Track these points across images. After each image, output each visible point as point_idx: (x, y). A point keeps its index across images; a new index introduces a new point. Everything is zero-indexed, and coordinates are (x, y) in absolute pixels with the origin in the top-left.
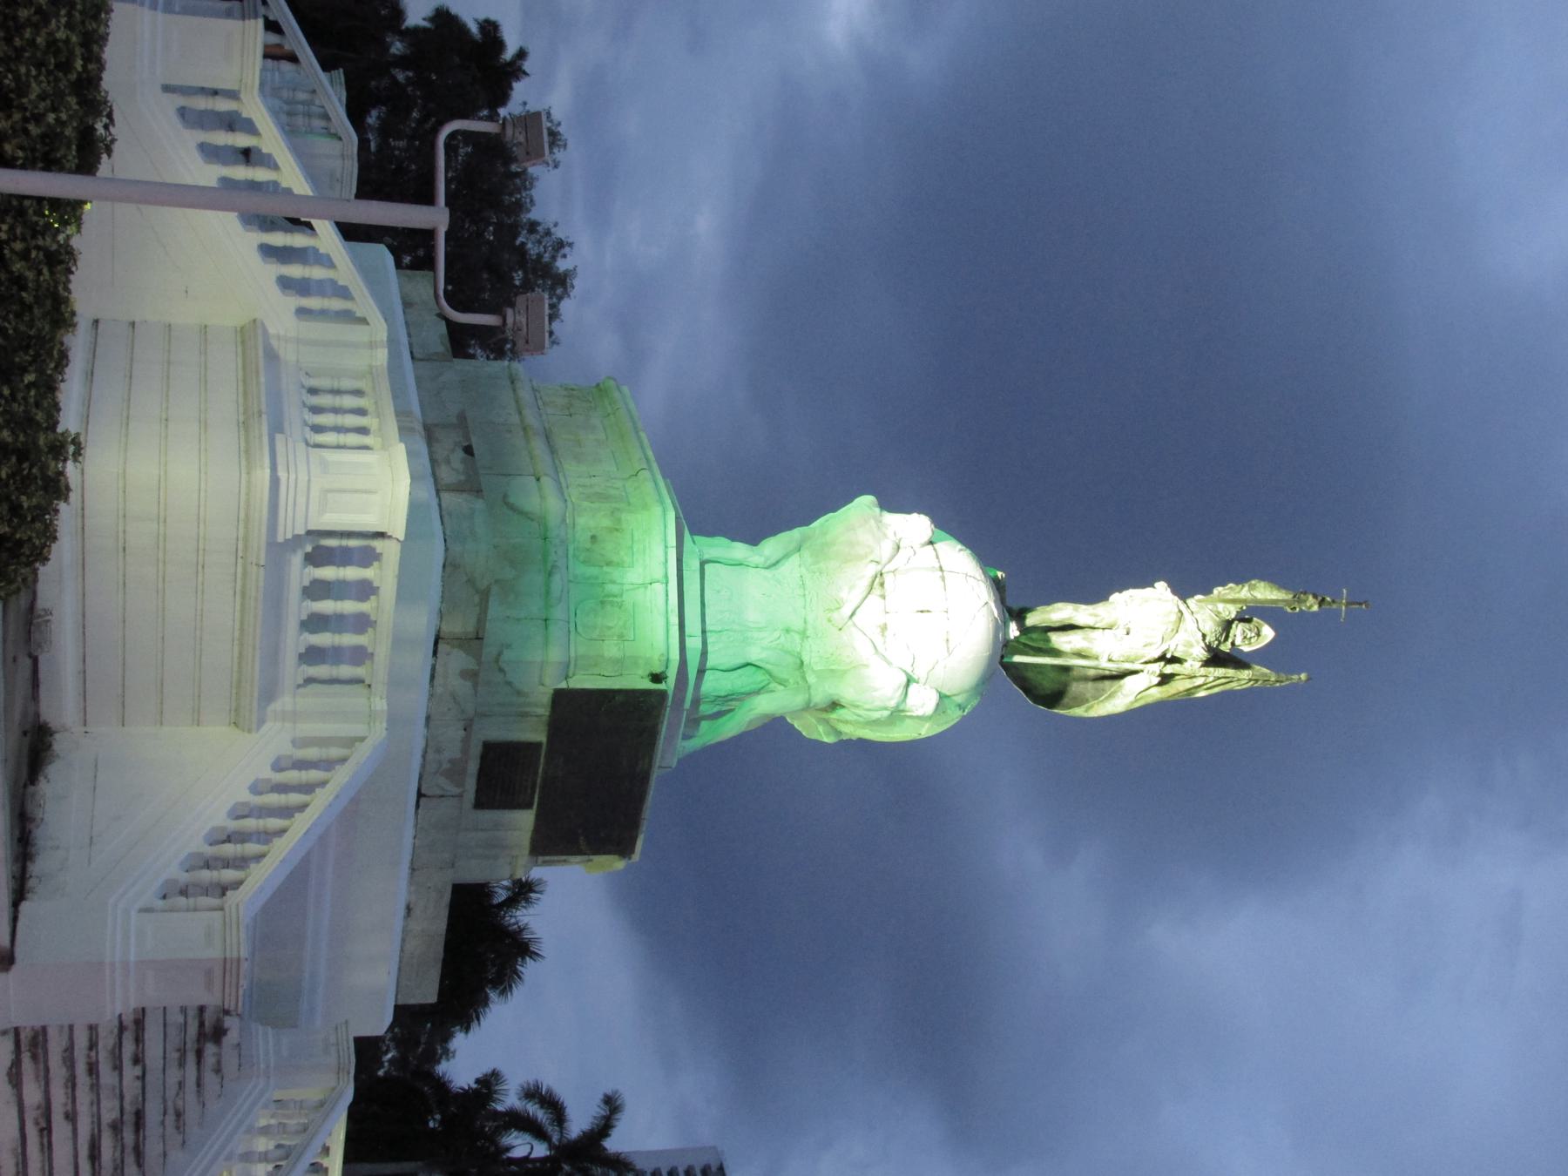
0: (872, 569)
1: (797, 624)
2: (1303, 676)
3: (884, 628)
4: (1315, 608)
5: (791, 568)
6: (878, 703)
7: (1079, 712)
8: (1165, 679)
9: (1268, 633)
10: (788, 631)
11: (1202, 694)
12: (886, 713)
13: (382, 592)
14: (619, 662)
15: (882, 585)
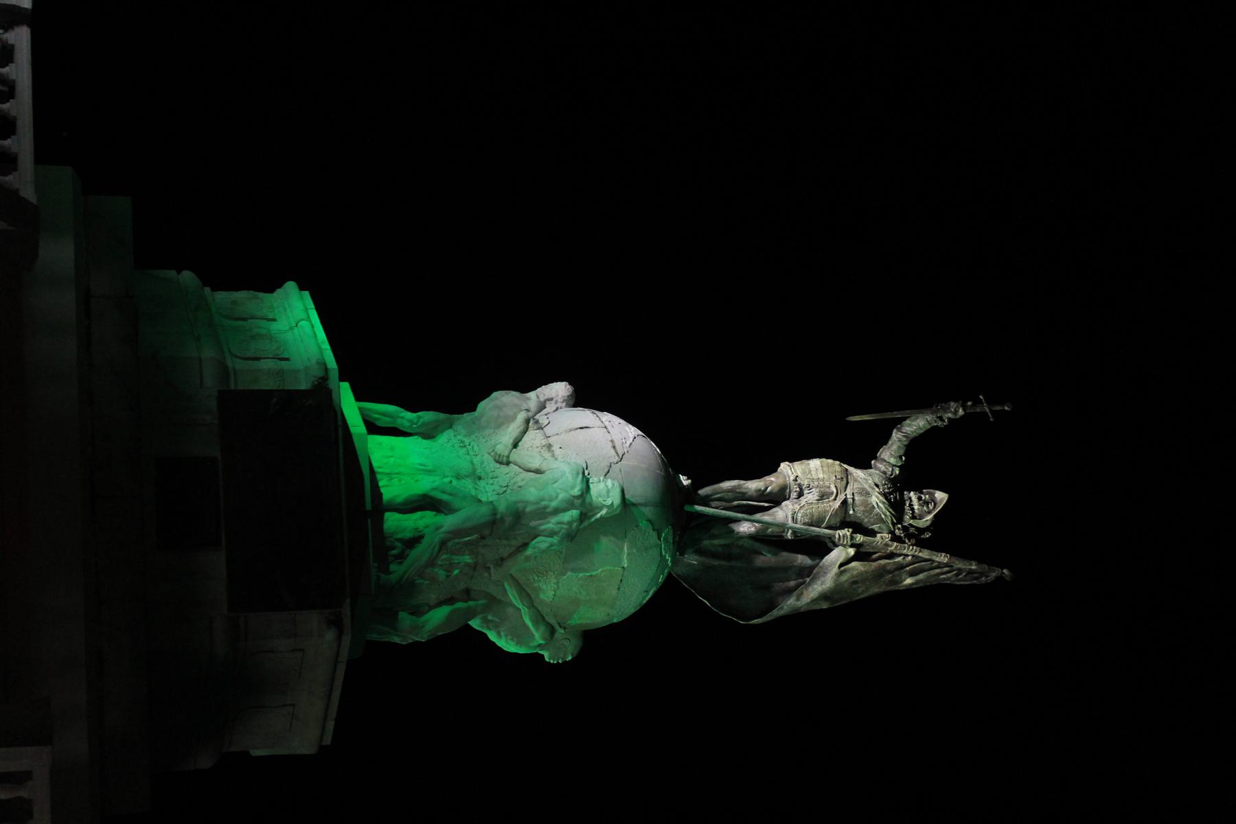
0: (521, 417)
1: (464, 465)
2: (1005, 571)
3: (549, 446)
4: (961, 412)
5: (445, 439)
6: (562, 496)
7: (790, 604)
8: (862, 555)
9: (941, 496)
10: (458, 477)
11: (909, 581)
12: (575, 513)
13: (19, 123)
14: (280, 373)
15: (537, 422)
